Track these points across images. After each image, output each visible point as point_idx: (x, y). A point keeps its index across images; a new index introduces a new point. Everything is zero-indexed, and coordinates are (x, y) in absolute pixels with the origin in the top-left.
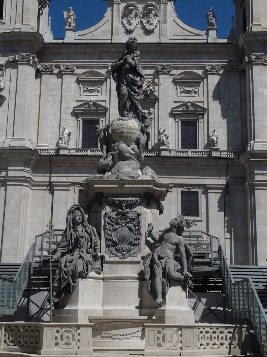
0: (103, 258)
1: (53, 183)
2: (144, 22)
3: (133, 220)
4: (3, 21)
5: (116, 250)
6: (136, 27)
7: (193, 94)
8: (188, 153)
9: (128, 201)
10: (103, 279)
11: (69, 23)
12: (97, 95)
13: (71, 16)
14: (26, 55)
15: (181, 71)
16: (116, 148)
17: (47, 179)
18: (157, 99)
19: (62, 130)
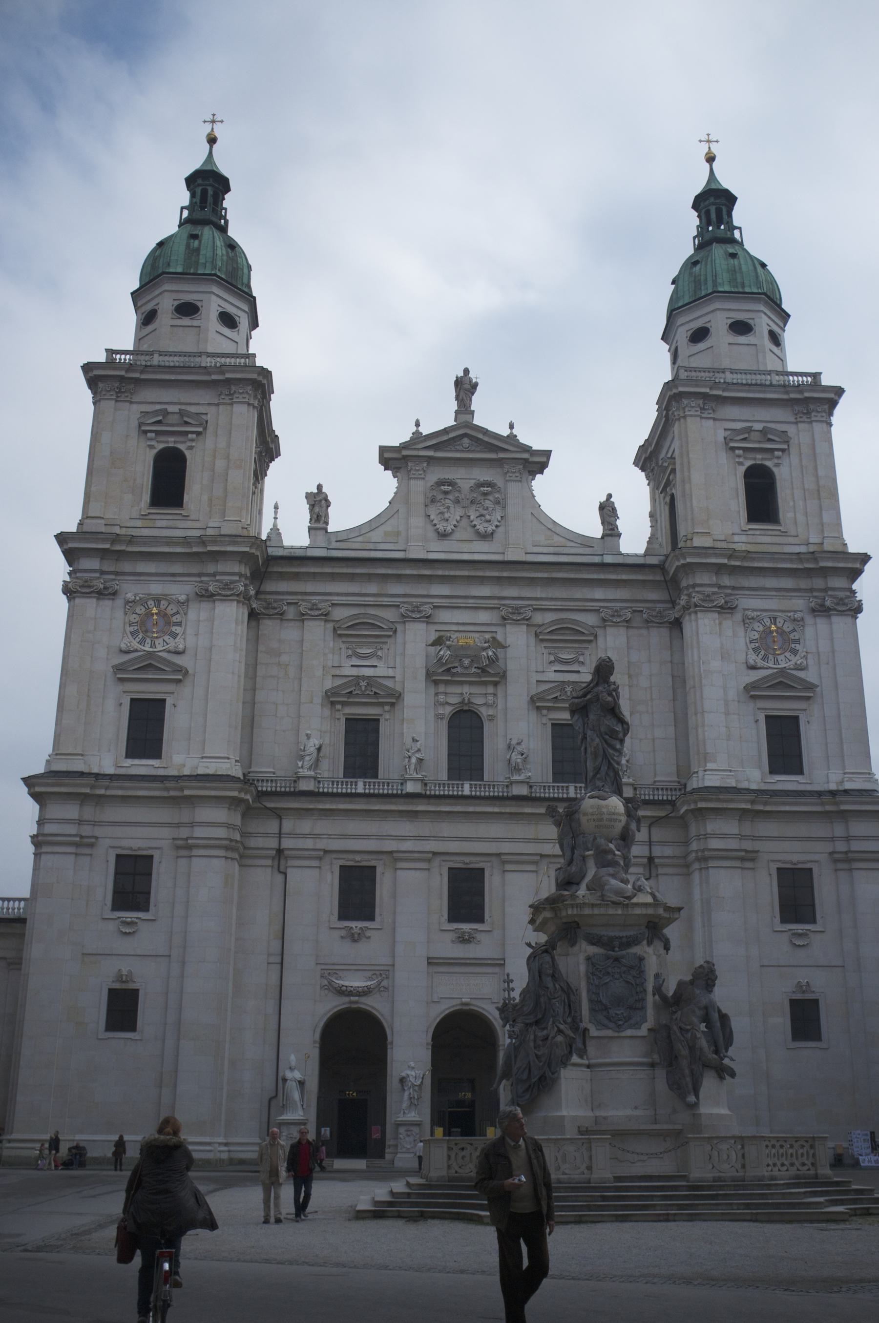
0: (586, 1030)
1: (286, 852)
2: (472, 518)
3: (632, 967)
4: (184, 513)
5: (609, 1018)
6: (455, 526)
7: (575, 667)
8: (567, 787)
9: (623, 937)
10: (588, 1066)
11: (318, 516)
12: (376, 666)
13: (320, 501)
14: (232, 582)
15: (549, 617)
16: (590, 846)
17: (273, 843)
18: (504, 676)
19: (303, 738)
